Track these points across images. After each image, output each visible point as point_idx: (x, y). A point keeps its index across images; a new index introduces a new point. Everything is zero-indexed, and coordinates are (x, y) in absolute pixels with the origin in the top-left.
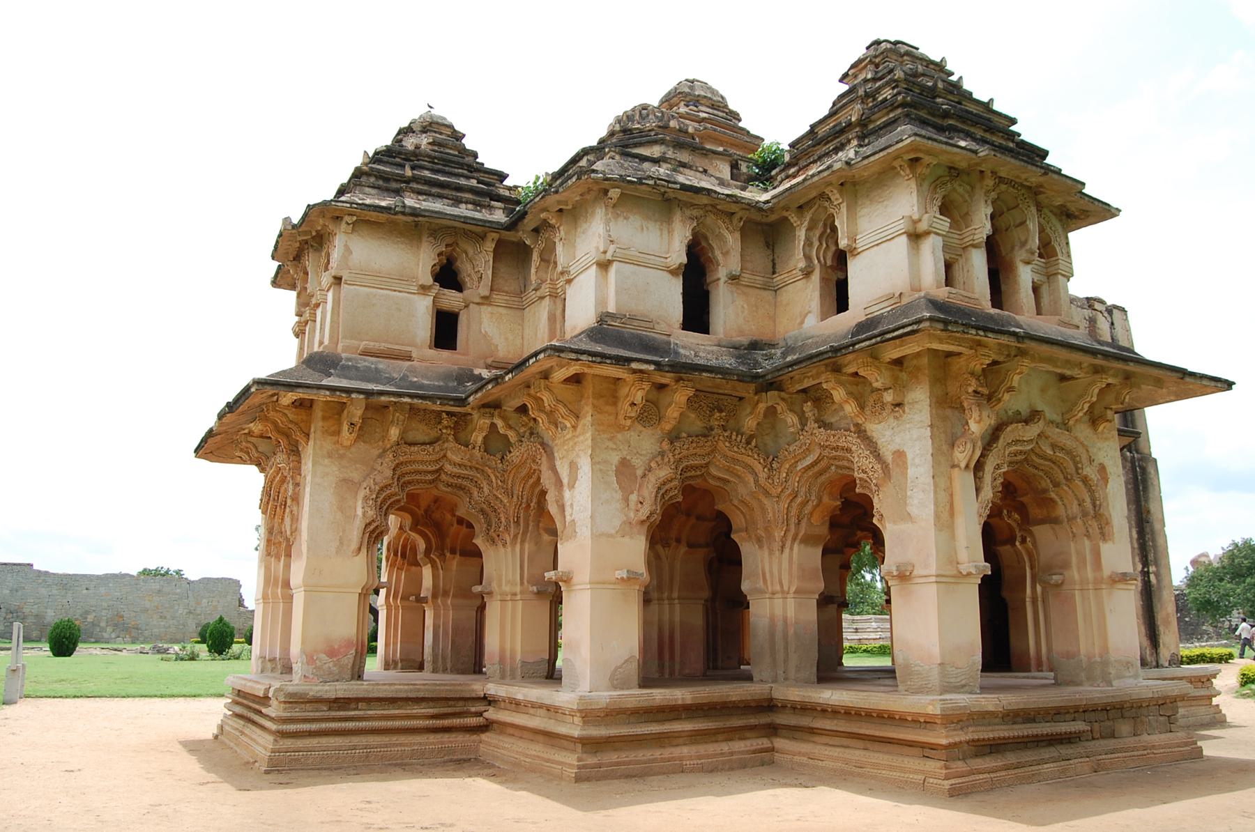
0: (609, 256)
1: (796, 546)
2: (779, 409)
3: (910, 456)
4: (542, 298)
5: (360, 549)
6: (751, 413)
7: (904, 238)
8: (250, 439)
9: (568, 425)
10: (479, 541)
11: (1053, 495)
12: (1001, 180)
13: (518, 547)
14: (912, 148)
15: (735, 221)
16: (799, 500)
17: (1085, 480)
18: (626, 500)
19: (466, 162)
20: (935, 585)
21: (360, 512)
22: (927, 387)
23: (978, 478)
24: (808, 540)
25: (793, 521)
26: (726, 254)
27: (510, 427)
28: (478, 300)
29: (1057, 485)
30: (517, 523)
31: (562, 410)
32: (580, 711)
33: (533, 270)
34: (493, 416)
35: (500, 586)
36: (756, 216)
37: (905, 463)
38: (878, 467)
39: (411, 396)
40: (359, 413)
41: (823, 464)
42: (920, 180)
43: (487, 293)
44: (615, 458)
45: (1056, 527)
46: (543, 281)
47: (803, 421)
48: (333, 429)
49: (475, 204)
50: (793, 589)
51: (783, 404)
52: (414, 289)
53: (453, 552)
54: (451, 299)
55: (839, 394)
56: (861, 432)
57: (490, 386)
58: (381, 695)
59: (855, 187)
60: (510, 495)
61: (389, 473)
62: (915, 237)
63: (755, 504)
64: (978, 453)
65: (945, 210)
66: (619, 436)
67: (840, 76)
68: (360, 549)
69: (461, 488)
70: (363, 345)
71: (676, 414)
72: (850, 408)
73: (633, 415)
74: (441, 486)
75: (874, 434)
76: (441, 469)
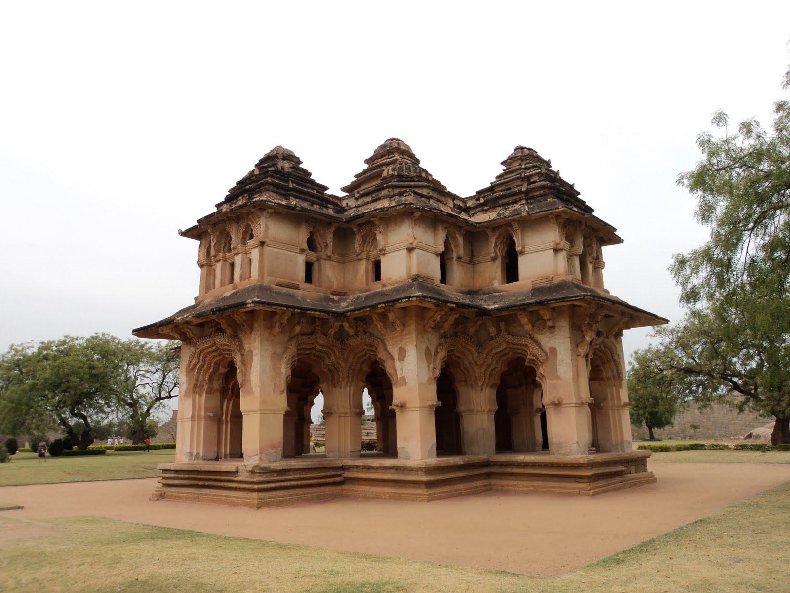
0: (414, 245)
4: (360, 260)
7: (552, 251)
8: (189, 326)
9: (399, 329)
12: (586, 226)
13: (348, 389)
14: (562, 212)
16: (491, 368)
17: (615, 361)
18: (428, 366)
20: (574, 408)
24: (492, 387)
26: (457, 246)
27: (351, 327)
28: (325, 257)
29: (604, 363)
31: (398, 322)
32: (425, 468)
33: (357, 245)
34: (343, 321)
38: (543, 354)
39: (321, 311)
41: (506, 351)
42: (559, 224)
43: (329, 254)
44: (424, 347)
46: (363, 251)
47: (499, 331)
49: (321, 205)
52: (298, 250)
54: (313, 256)
55: (524, 320)
56: (532, 338)
57: (368, 309)
59: (529, 223)
60: (345, 361)
62: (556, 250)
67: (502, 161)
68: (283, 391)
69: (320, 357)
70: (278, 280)
72: (528, 327)
73: (433, 326)
75: (538, 339)
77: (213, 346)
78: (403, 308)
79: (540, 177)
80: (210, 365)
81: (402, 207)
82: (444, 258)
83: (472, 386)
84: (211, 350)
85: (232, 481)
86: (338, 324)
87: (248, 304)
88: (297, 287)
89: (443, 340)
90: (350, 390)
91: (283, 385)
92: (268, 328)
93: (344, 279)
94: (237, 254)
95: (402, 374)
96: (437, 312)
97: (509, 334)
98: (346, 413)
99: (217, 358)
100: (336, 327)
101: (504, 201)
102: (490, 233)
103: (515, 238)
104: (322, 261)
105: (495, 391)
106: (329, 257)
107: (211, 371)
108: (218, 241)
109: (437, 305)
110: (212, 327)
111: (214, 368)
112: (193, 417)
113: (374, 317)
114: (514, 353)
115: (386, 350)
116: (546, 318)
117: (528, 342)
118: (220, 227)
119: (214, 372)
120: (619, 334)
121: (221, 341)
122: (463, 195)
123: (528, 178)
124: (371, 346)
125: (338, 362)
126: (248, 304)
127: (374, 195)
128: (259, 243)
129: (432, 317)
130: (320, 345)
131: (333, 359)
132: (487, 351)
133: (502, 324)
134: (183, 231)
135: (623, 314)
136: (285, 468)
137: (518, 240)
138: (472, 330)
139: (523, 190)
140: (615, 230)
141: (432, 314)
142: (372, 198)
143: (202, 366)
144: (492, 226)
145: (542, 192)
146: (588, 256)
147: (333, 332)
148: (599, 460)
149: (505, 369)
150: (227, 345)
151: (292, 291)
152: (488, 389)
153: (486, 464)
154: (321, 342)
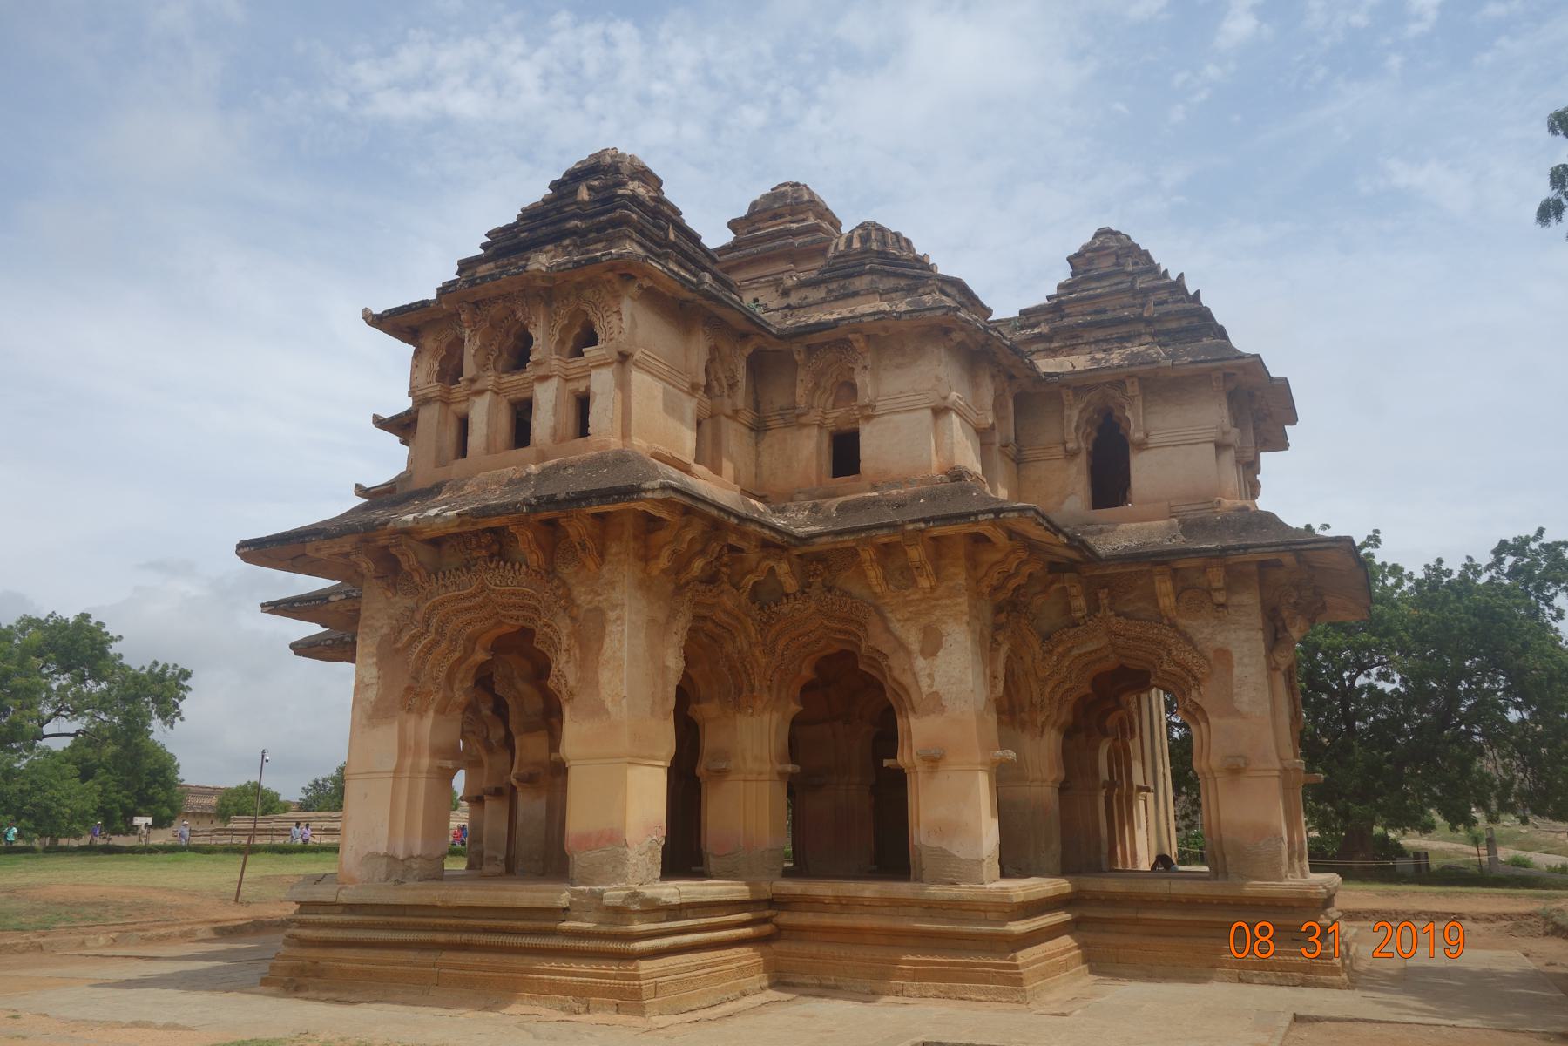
0: (948, 403)
3: (1236, 656)
7: (1212, 446)
31: (929, 568)
47: (1094, 606)
62: (1220, 447)
72: (1167, 602)
77: (474, 596)
79: (1172, 293)
81: (939, 313)
83: (1023, 726)
84: (467, 604)
85: (553, 933)
87: (646, 491)
93: (758, 465)
94: (544, 378)
97: (1118, 615)
98: (760, 774)
99: (478, 626)
101: (1100, 334)
102: (1067, 396)
104: (723, 418)
106: (736, 411)
107: (456, 655)
108: (483, 346)
110: (479, 546)
112: (397, 772)
113: (867, 555)
115: (888, 630)
118: (496, 310)
119: (460, 661)
121: (504, 584)
126: (646, 491)
127: (834, 286)
128: (616, 356)
130: (726, 612)
132: (1060, 649)
134: (379, 312)
136: (685, 899)
140: (1293, 420)
141: (997, 556)
142: (829, 291)
143: (435, 643)
144: (1077, 385)
149: (1086, 689)
150: (523, 595)
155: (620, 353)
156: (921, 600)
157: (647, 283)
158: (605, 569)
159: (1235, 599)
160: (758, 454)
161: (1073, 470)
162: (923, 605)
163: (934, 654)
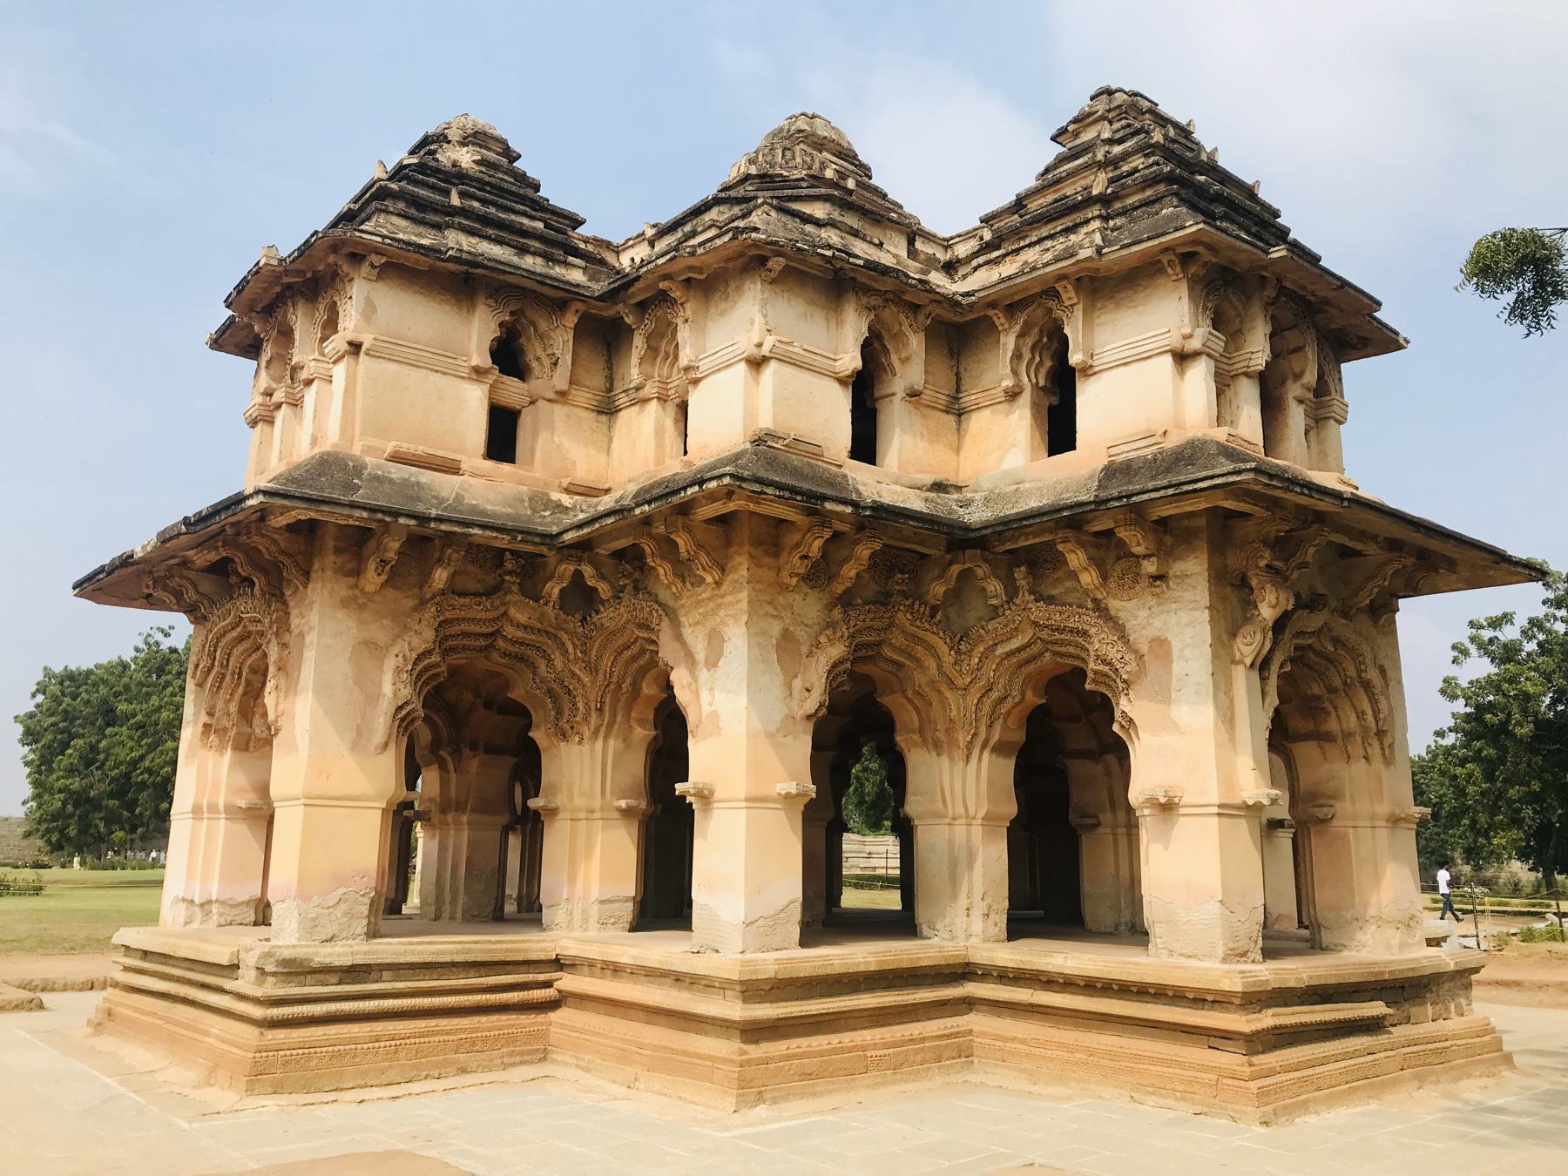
0: (765, 351)
1: (986, 755)
2: (980, 572)
3: (1176, 647)
4: (646, 401)
5: (386, 745)
6: (940, 577)
8: (185, 572)
9: (709, 579)
10: (537, 735)
11: (1327, 705)
12: (1282, 290)
13: (599, 744)
14: (1195, 240)
15: (921, 318)
16: (995, 695)
18: (790, 687)
19: (525, 192)
21: (387, 688)
22: (1204, 557)
23: (1263, 679)
24: (1000, 749)
25: (984, 721)
27: (603, 577)
28: (552, 396)
29: (1332, 690)
30: (600, 710)
31: (704, 558)
32: (742, 982)
33: (635, 359)
35: (571, 799)
36: (948, 315)
37: (1168, 654)
39: (483, 527)
40: (396, 545)
41: (1035, 649)
42: (1193, 283)
43: (564, 386)
44: (776, 628)
45: (1326, 745)
47: (1012, 591)
48: (349, 566)
49: (548, 258)
50: (982, 813)
51: (986, 567)
53: (474, 747)
54: (513, 391)
55: (1076, 558)
56: (1100, 609)
58: (409, 959)
59: (1104, 286)
60: (593, 669)
61: (430, 634)
62: (1182, 358)
63: (934, 698)
64: (1268, 646)
65: (1216, 324)
66: (781, 599)
67: (1054, 131)
69: (522, 659)
70: (390, 447)
71: (853, 573)
72: (1089, 578)
73: (802, 571)
74: (495, 656)
75: (1121, 614)
76: (498, 631)
78: (722, 520)
80: (240, 674)
82: (865, 393)
83: (938, 747)
84: (234, 634)
85: (220, 990)
86: (568, 569)
88: (453, 469)
89: (837, 613)
90: (605, 748)
91: (381, 723)
92: (348, 574)
95: (711, 704)
96: (809, 530)
98: (593, 811)
100: (561, 577)
102: (1000, 320)
103: (1067, 331)
105: (1008, 766)
106: (562, 394)
107: (241, 690)
109: (811, 513)
111: (248, 683)
113: (648, 547)
114: (1055, 653)
115: (679, 637)
116: (1137, 550)
117: (1089, 622)
120: (1382, 611)
122: (943, 232)
123: (1112, 163)
124: (648, 628)
125: (574, 674)
128: (346, 347)
129: (798, 545)
131: (559, 663)
133: (1020, 574)
135: (1394, 545)
136: (360, 960)
137: (1075, 330)
138: (938, 590)
139: (1095, 192)
145: (1149, 193)
146: (1289, 382)
147: (556, 591)
148: (1292, 984)
149: (1033, 699)
151: (426, 477)
152: (986, 755)
153: (964, 972)
154: (522, 618)
155: (350, 343)
156: (709, 599)
157: (378, 260)
158: (310, 586)
159: (1178, 568)
160: (610, 440)
161: (1015, 416)
162: (711, 605)
163: (715, 665)
